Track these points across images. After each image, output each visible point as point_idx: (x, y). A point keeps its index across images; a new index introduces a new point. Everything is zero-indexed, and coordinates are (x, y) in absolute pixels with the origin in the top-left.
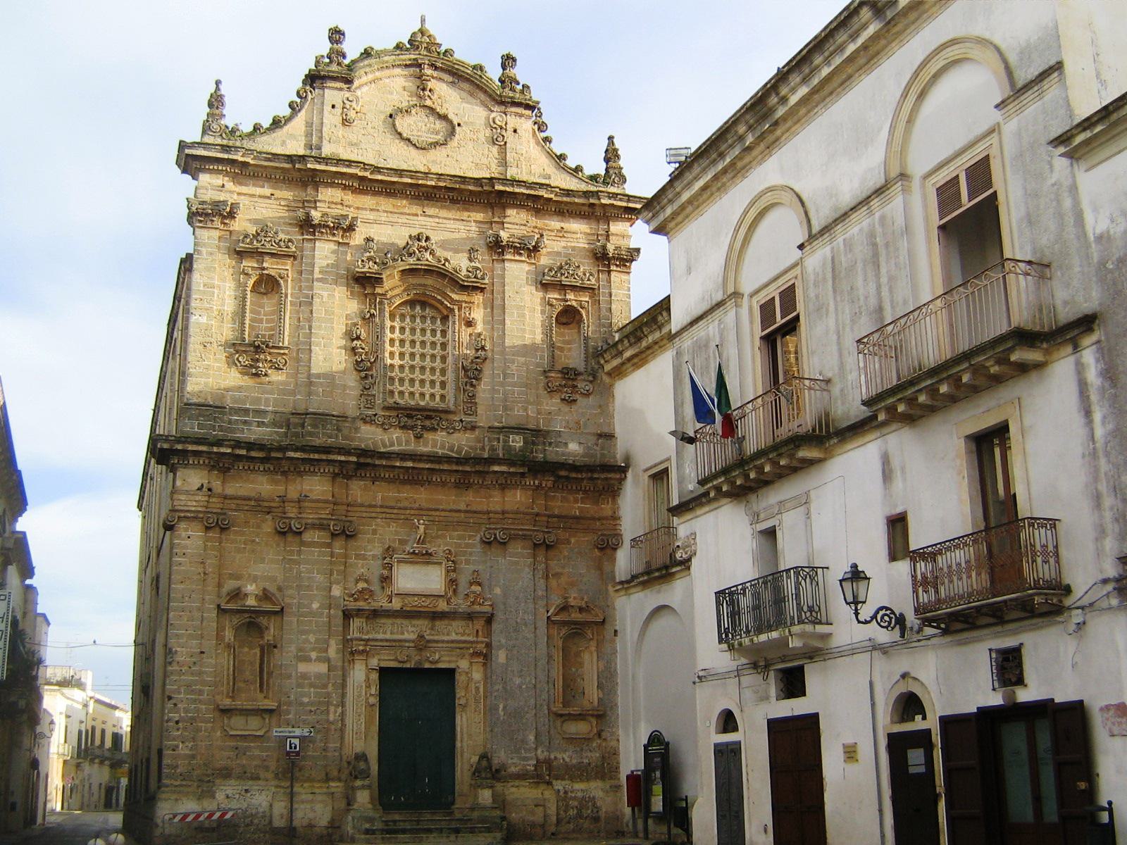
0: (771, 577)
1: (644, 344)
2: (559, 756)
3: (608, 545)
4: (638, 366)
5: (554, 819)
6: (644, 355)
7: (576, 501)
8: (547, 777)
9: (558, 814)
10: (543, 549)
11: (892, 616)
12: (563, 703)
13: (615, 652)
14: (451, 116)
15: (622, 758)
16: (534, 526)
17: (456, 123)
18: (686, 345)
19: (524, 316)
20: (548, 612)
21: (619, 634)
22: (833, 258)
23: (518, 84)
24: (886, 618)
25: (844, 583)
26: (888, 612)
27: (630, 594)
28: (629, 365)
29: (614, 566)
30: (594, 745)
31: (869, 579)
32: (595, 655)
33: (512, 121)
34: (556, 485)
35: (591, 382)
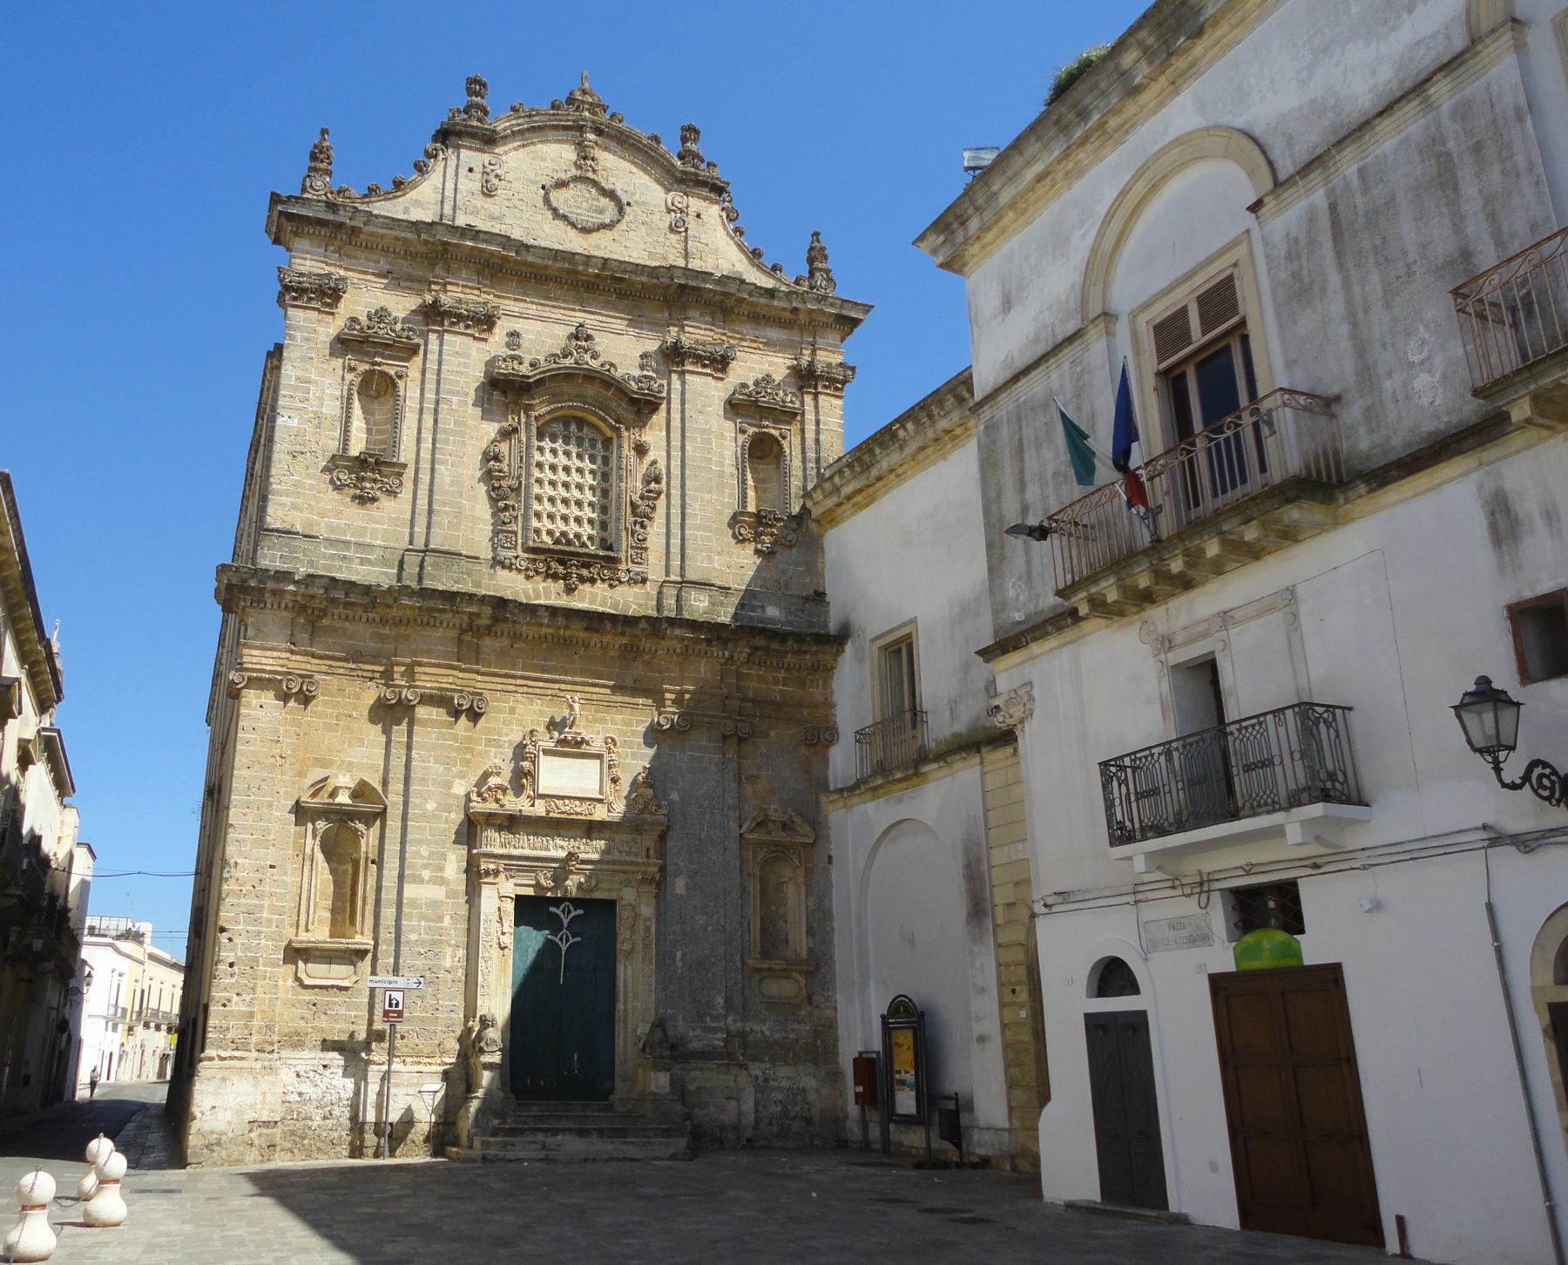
0: (1181, 742)
1: (874, 472)
2: (756, 1028)
3: (820, 735)
4: (860, 507)
5: (752, 1118)
6: (871, 490)
7: (776, 681)
8: (741, 1058)
9: (757, 1111)
10: (734, 741)
11: (1553, 778)
12: (761, 953)
13: (829, 886)
14: (619, 193)
15: (842, 1032)
16: (723, 712)
17: (624, 201)
18: (1004, 413)
19: (709, 442)
20: (741, 827)
21: (834, 861)
22: (1333, 208)
23: (702, 161)
24: (1546, 782)
25: (1465, 715)
26: (1547, 771)
27: (851, 806)
28: (847, 506)
29: (827, 768)
30: (803, 1012)
31: (1518, 705)
32: (803, 888)
33: (695, 204)
34: (751, 659)
35: (794, 530)
